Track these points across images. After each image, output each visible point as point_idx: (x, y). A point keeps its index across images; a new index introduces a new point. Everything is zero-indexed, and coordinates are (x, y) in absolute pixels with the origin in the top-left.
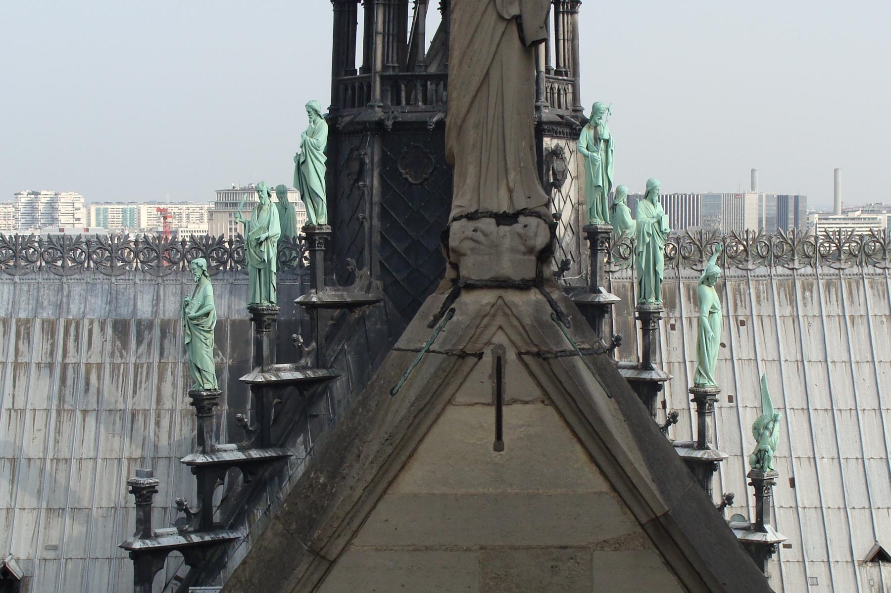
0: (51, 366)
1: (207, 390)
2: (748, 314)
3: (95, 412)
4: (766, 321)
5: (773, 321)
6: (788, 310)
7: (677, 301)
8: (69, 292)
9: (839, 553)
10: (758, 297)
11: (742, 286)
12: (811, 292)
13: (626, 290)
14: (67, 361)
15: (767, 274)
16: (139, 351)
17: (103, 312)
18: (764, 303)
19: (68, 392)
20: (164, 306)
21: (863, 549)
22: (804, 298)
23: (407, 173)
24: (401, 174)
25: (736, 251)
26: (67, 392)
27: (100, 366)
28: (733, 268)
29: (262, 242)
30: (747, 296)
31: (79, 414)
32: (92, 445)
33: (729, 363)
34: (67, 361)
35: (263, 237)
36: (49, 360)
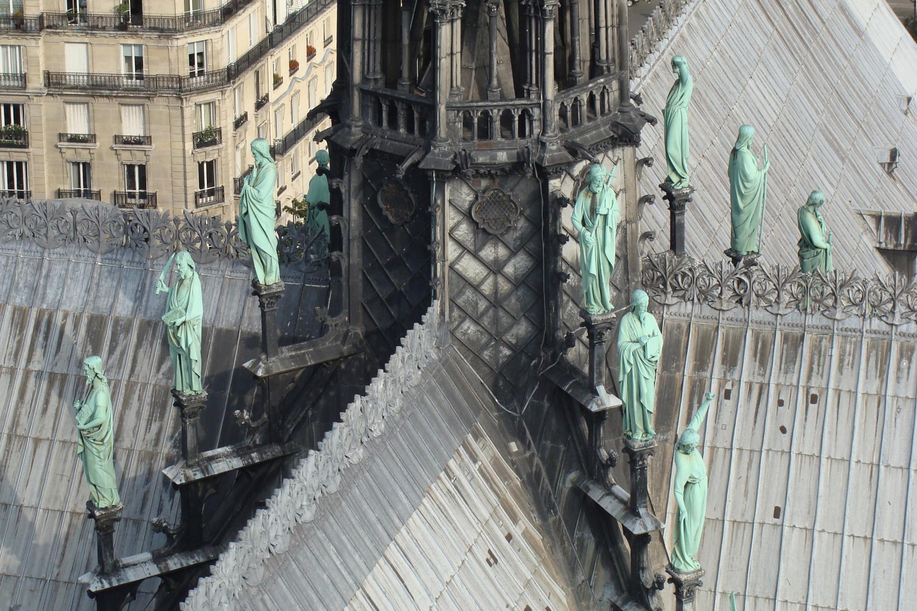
0: (12, 372)
1: (102, 509)
2: (824, 386)
3: (47, 443)
4: (845, 397)
5: (853, 399)
7: (740, 355)
8: (49, 271)
10: (841, 361)
11: (824, 342)
12: (910, 361)
13: (680, 333)
14: (31, 367)
15: (858, 327)
16: (110, 362)
17: (80, 302)
18: (847, 370)
19: (24, 410)
20: (148, 301)
22: (899, 369)
23: (387, 209)
24: (381, 210)
25: (822, 293)
26: (24, 410)
27: (64, 377)
28: (817, 315)
29: (178, 327)
30: (827, 358)
31: (30, 444)
32: (36, 489)
33: (785, 457)
34: (31, 367)
35: (179, 322)
36: (12, 364)
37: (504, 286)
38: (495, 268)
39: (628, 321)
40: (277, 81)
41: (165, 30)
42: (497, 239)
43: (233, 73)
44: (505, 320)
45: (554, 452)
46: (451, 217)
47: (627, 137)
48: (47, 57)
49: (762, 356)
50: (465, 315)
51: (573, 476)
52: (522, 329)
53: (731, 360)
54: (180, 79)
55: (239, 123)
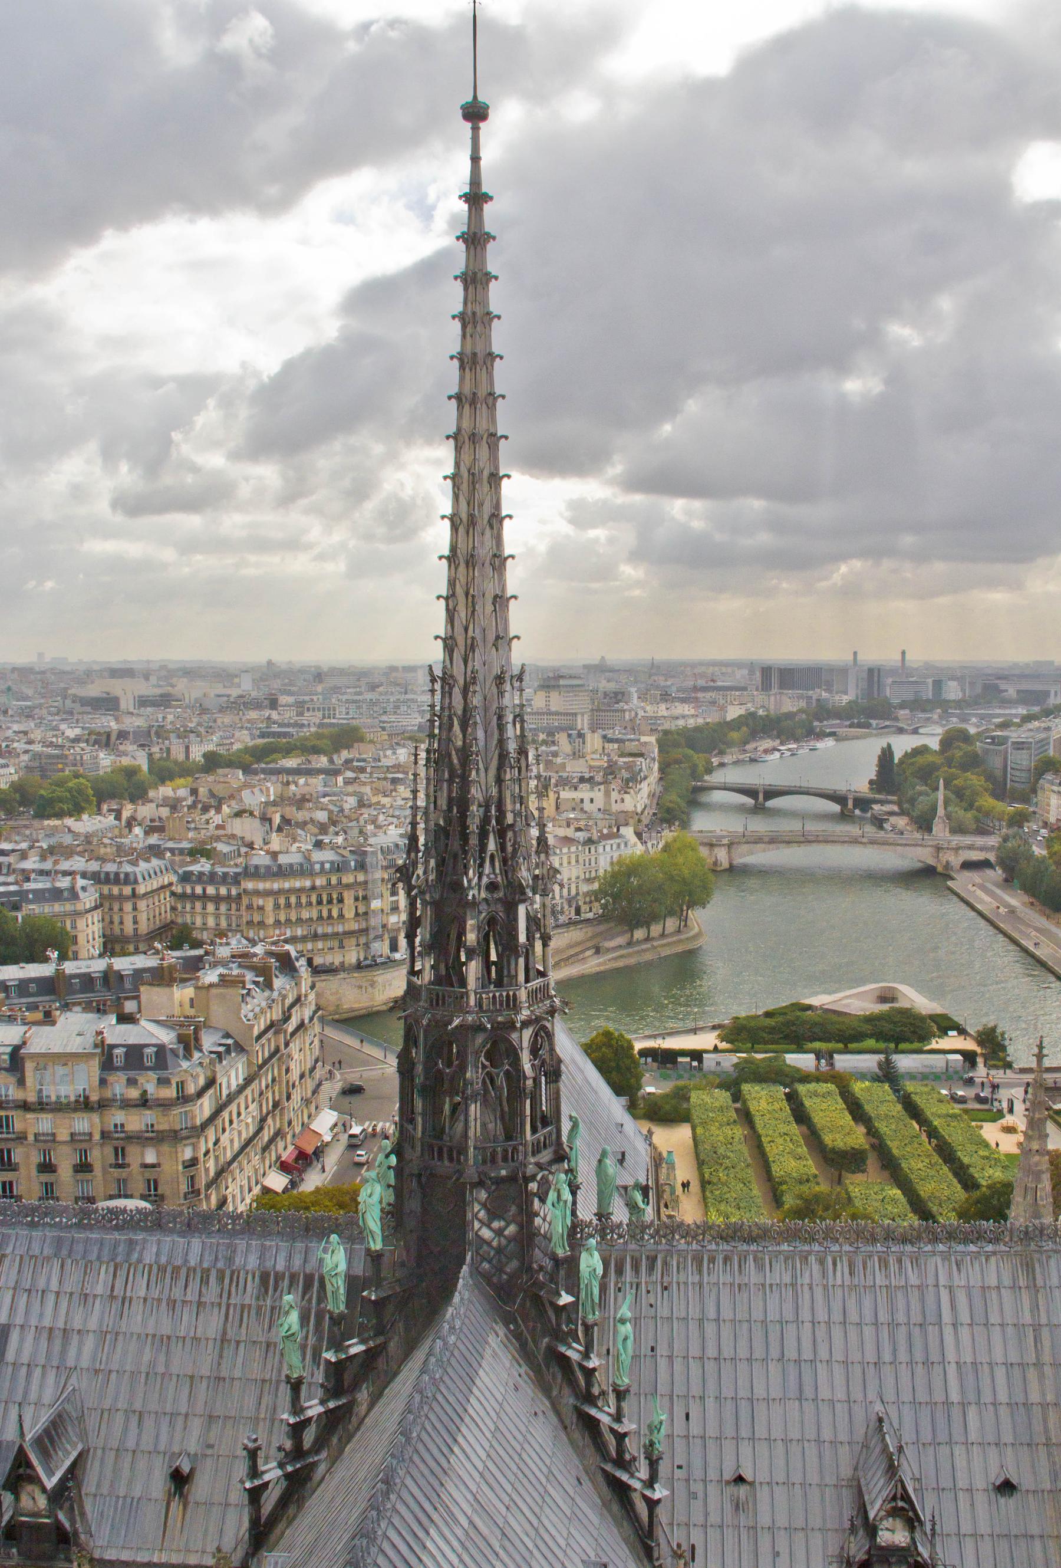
0: (220, 1304)
4: (682, 1287)
6: (697, 1279)
9: (713, 1475)
21: (728, 1475)
27: (250, 1306)
37: (504, 1241)
38: (499, 1232)
39: (584, 1256)
40: (224, 1130)
41: (165, 1105)
42: (499, 1217)
43: (204, 1126)
44: (504, 1260)
45: (534, 1328)
46: (477, 1207)
47: (560, 1157)
48: (102, 1122)
49: (636, 1268)
50: (484, 1259)
51: (546, 1340)
52: (514, 1264)
53: (620, 1271)
54: (176, 1132)
55: (207, 1153)
